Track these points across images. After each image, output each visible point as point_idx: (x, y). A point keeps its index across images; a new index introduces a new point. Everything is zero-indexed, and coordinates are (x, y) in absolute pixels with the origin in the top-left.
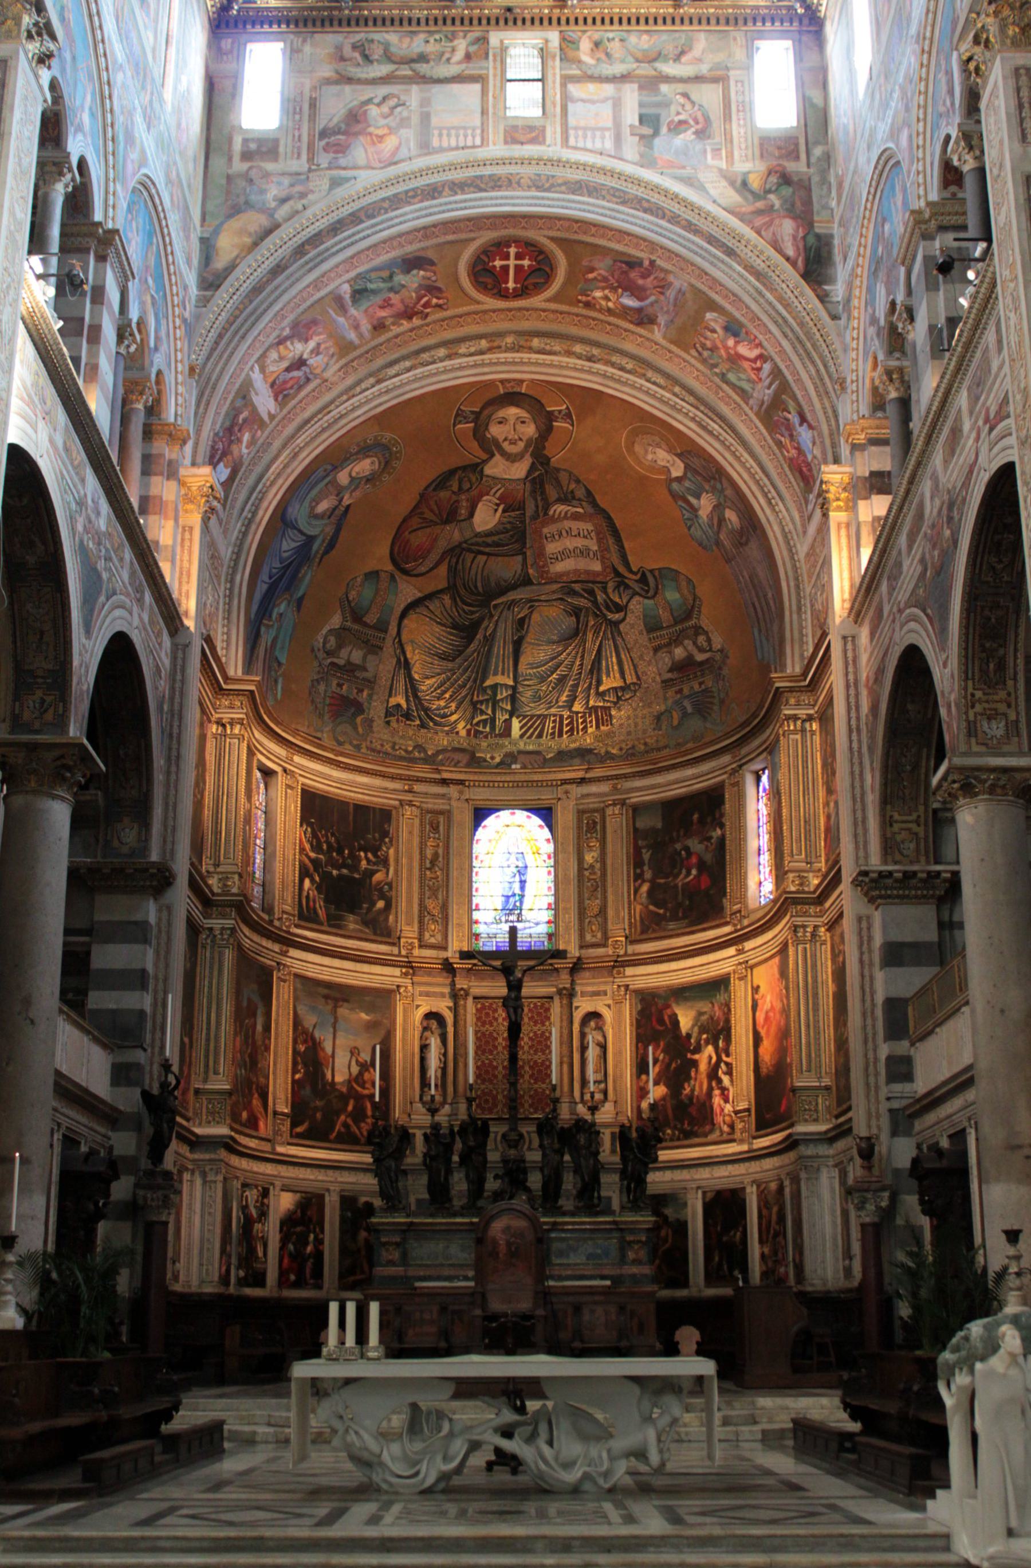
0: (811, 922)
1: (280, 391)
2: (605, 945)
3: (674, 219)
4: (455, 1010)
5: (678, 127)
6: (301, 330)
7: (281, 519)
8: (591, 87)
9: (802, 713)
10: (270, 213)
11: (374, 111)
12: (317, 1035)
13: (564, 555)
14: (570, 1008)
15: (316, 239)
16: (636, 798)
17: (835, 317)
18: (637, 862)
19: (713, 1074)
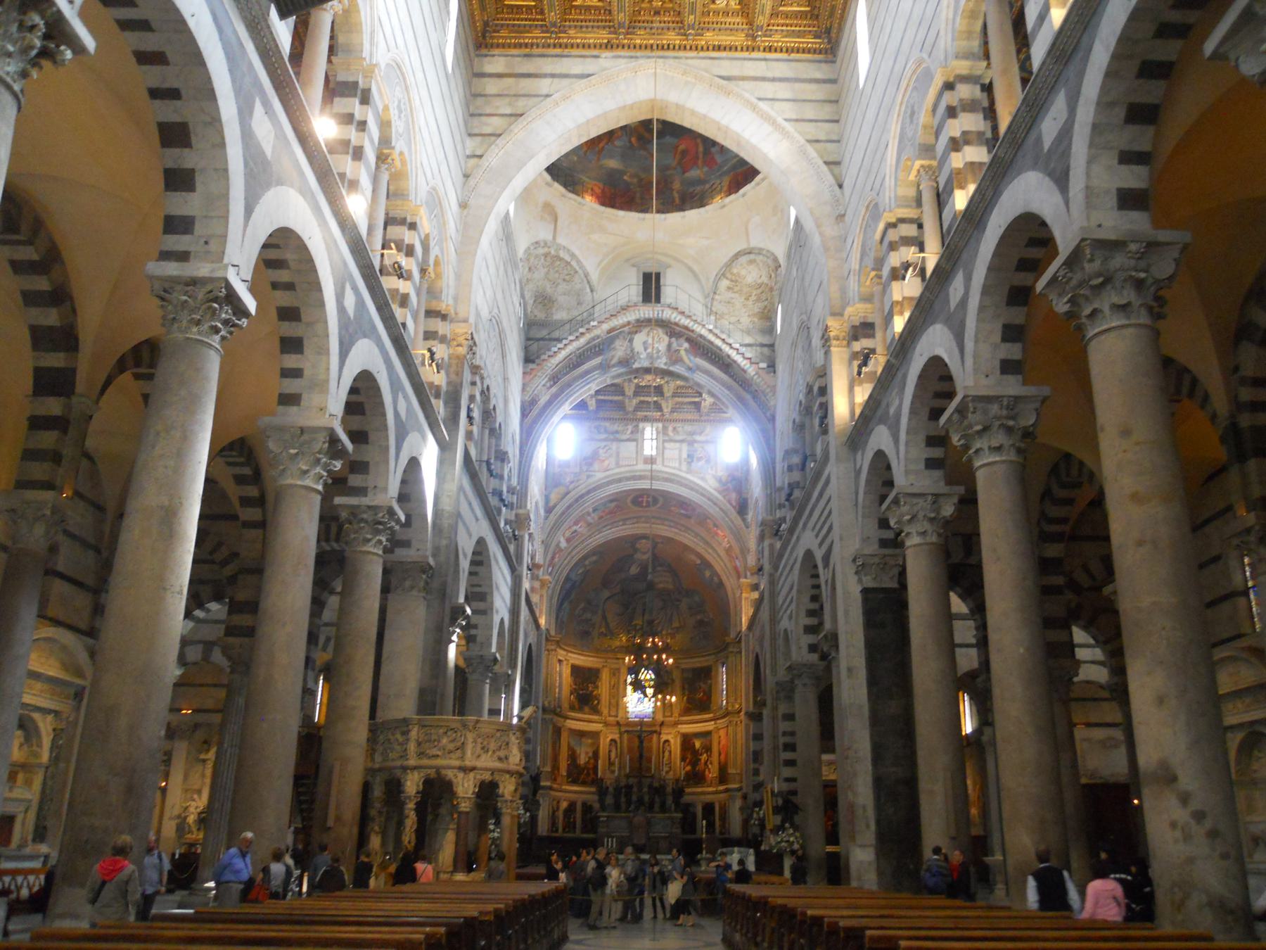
0: (736, 719)
1: (568, 540)
2: (671, 716)
3: (697, 491)
4: (620, 738)
5: (699, 459)
6: (576, 523)
7: (567, 579)
8: (672, 445)
9: (735, 650)
10: (568, 487)
11: (601, 451)
12: (576, 748)
13: (661, 582)
14: (659, 739)
15: (582, 496)
16: (683, 666)
17: (747, 527)
18: (683, 689)
19: (706, 763)
